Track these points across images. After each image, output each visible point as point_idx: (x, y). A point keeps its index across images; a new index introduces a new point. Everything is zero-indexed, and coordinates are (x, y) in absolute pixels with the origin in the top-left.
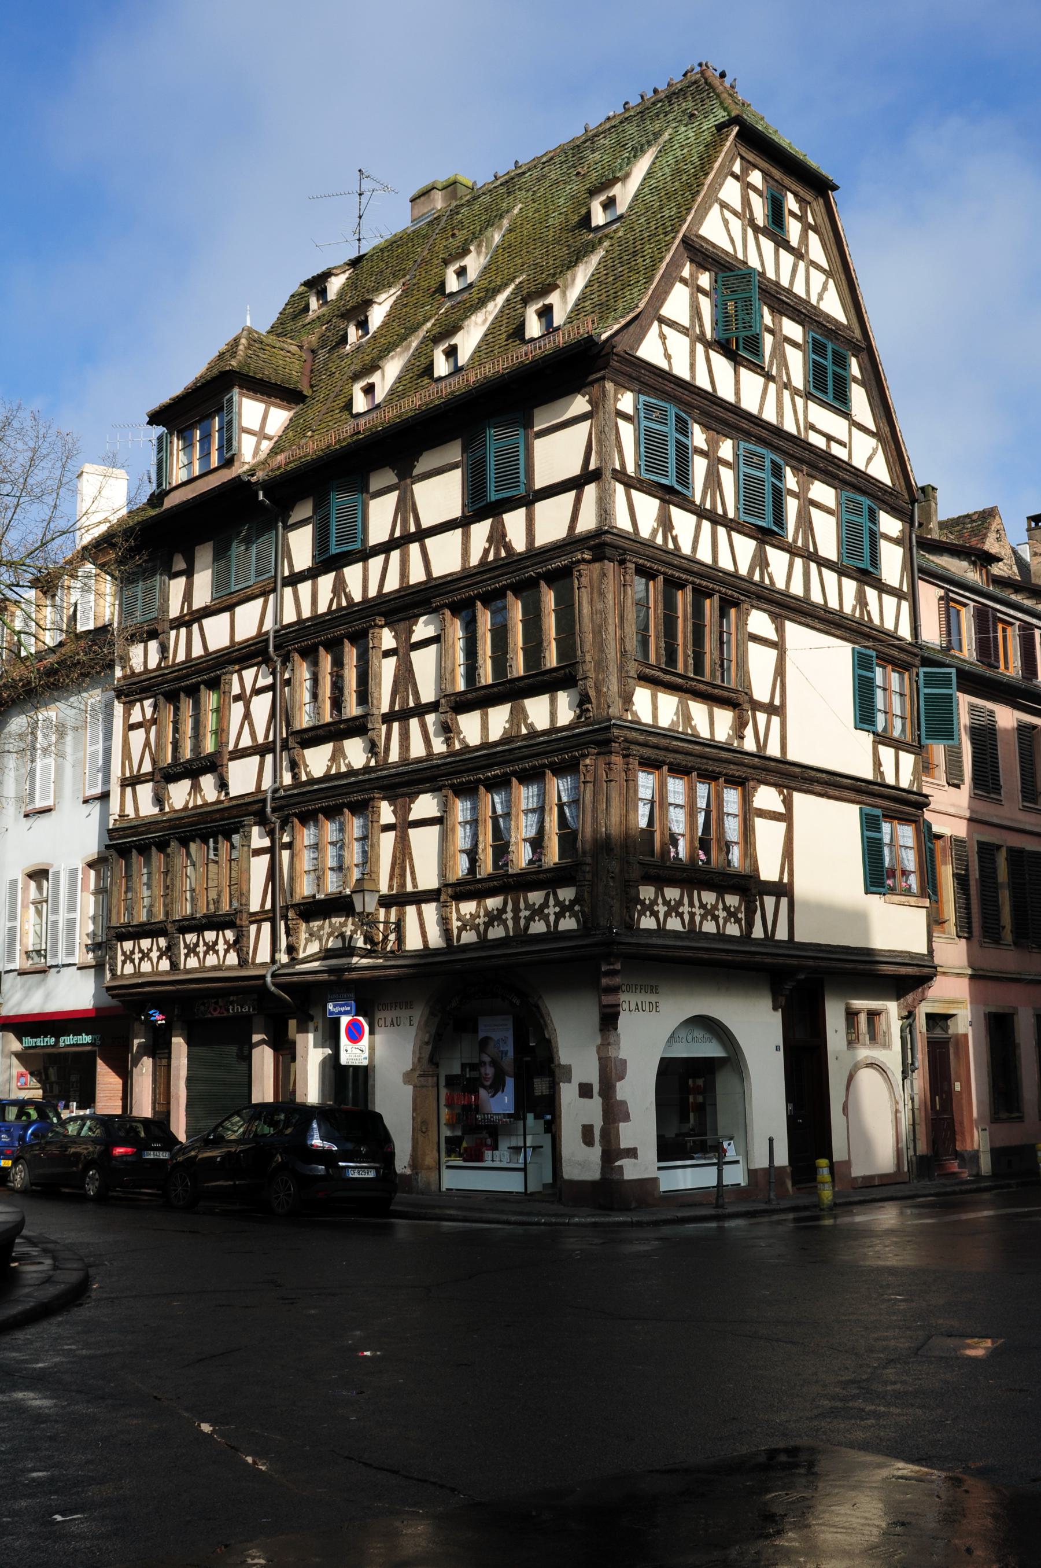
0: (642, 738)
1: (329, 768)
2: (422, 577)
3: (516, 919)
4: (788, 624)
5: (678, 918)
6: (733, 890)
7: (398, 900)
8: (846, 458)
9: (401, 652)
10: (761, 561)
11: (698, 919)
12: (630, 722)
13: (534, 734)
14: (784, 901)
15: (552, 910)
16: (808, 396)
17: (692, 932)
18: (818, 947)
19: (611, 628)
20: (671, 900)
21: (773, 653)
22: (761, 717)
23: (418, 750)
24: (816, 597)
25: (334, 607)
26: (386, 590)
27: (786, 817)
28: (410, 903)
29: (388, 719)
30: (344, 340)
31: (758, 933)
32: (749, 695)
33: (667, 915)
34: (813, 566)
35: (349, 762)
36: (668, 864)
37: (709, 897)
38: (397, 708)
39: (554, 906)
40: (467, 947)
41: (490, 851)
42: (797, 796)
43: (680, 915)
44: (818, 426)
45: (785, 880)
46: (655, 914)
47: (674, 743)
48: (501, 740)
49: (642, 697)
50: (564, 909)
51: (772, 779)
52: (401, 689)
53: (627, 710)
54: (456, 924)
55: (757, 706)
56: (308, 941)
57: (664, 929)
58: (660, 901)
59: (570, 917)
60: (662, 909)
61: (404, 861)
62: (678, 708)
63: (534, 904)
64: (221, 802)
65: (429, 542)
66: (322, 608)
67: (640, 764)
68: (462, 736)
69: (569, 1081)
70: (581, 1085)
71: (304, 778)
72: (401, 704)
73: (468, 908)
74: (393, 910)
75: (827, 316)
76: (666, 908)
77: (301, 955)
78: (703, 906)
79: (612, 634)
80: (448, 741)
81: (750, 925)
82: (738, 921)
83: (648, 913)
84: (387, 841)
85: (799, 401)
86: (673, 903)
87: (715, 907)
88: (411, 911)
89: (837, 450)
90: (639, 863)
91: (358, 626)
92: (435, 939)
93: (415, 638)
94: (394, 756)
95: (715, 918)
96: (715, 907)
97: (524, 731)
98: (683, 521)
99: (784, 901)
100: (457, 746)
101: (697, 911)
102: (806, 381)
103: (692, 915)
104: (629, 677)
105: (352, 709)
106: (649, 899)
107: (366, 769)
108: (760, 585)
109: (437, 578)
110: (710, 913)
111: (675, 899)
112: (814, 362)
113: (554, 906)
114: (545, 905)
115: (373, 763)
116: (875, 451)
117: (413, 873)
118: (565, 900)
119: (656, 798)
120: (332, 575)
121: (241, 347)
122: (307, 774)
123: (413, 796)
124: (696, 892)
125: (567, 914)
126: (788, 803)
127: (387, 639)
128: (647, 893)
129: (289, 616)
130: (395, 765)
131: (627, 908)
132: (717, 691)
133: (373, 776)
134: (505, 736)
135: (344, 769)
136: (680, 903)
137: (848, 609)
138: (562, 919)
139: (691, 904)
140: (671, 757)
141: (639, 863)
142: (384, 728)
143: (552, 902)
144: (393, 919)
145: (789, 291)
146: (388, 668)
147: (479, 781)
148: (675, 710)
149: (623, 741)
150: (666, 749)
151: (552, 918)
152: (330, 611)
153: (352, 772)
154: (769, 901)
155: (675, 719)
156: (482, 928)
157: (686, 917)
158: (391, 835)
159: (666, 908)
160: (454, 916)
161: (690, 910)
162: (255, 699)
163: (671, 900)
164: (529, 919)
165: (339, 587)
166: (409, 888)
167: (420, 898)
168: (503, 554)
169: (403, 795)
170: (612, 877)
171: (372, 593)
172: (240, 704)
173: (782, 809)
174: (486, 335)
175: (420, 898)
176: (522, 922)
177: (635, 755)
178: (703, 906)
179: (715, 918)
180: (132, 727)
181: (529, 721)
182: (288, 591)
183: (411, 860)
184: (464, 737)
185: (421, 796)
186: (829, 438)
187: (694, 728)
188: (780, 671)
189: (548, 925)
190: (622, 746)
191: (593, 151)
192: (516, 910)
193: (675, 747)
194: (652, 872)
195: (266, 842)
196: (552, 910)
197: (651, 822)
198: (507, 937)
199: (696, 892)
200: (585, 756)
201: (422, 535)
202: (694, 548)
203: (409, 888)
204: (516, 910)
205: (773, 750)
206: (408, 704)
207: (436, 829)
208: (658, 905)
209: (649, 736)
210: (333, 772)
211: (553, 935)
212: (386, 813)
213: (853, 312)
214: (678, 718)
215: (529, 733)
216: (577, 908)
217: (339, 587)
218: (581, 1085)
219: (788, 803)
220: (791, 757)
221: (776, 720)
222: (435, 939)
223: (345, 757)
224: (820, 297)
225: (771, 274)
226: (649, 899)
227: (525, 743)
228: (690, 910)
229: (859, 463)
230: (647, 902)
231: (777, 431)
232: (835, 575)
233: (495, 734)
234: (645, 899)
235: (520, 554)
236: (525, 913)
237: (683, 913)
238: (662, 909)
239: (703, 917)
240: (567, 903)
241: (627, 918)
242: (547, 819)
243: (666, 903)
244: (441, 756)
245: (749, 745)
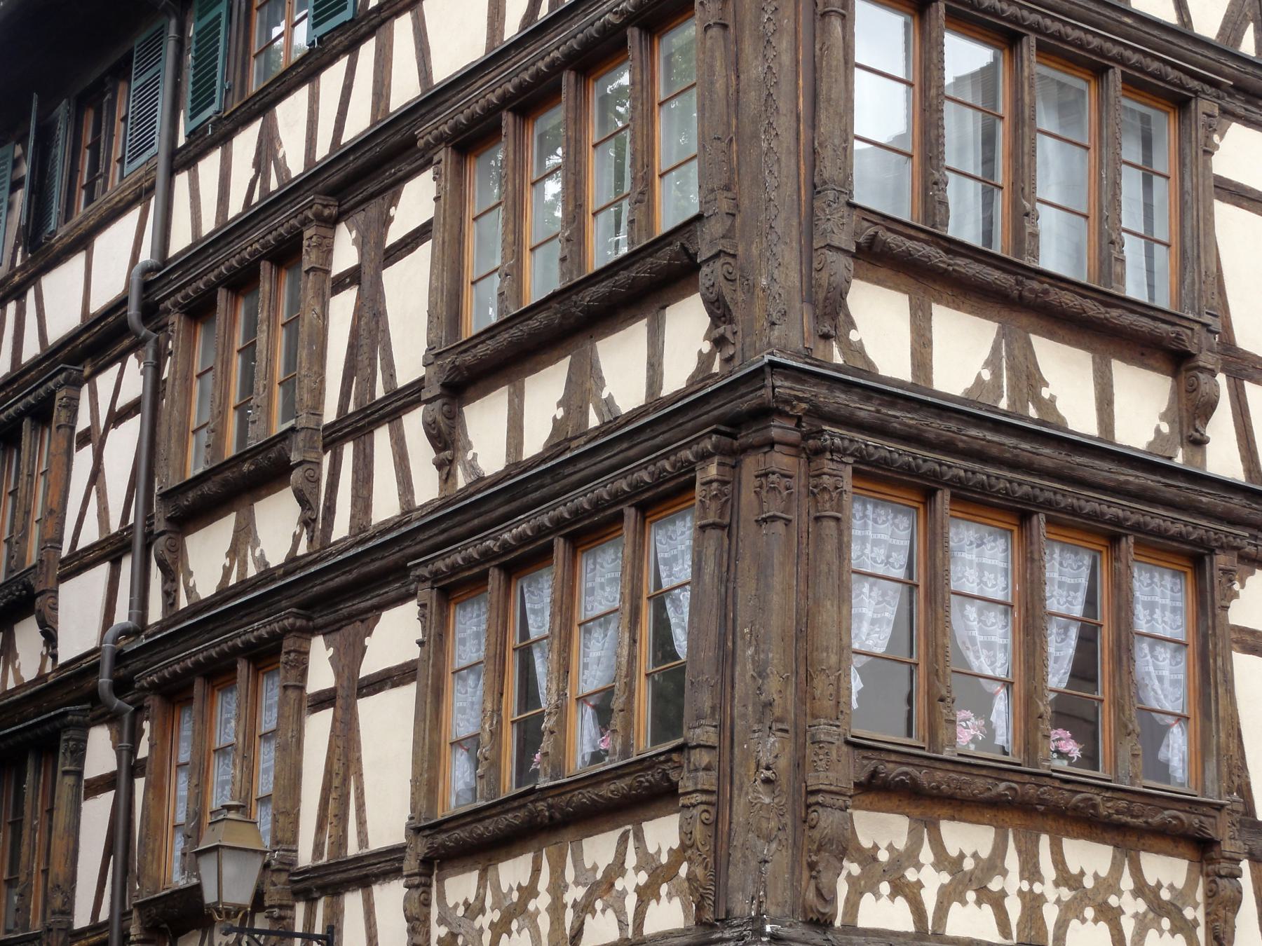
0: (866, 410)
5: (987, 909)
11: (1050, 914)
12: (838, 368)
19: (784, 124)
20: (962, 856)
29: (333, 438)
33: (947, 897)
35: (262, 555)
36: (946, 754)
38: (351, 409)
39: (637, 869)
47: (974, 432)
48: (546, 449)
50: (659, 875)
53: (826, 337)
57: (939, 936)
58: (926, 855)
59: (670, 896)
60: (931, 881)
61: (345, 781)
62: (996, 349)
63: (595, 868)
67: (857, 473)
68: (470, 456)
76: (945, 878)
78: (1066, 878)
79: (787, 138)
80: (445, 467)
83: (885, 887)
86: (968, 864)
87: (1110, 885)
90: (848, 743)
96: (1110, 885)
97: (594, 421)
101: (1047, 888)
103: (1033, 903)
104: (830, 247)
106: (890, 848)
111: (975, 855)
113: (637, 869)
114: (617, 868)
118: (659, 851)
119: (919, 578)
123: (369, 618)
124: (1045, 841)
125: (664, 889)
131: (812, 866)
132: (1115, 313)
134: (556, 440)
136: (994, 865)
138: (653, 903)
139: (1031, 871)
140: (958, 467)
141: (848, 743)
143: (631, 859)
148: (986, 352)
149: (808, 413)
150: (947, 447)
155: (987, 375)
157: (1014, 908)
159: (945, 878)
161: (1025, 886)
163: (962, 856)
170: (767, 781)
171: (323, 150)
177: (843, 451)
178: (1066, 878)
181: (605, 395)
184: (475, 455)
185: (387, 616)
187: (1048, 405)
190: (805, 427)
193: (977, 445)
194: (893, 770)
199: (1045, 841)
200: (704, 456)
204: (557, 888)
206: (373, 394)
208: (918, 866)
209: (892, 405)
214: (996, 375)
215: (604, 424)
216: (683, 870)
226: (890, 848)
228: (1025, 886)
230: (883, 856)
234: (876, 847)
236: (575, 894)
237: (1003, 894)
238: (931, 881)
239: (1070, 911)
240: (664, 859)
241: (811, 895)
243: (943, 861)
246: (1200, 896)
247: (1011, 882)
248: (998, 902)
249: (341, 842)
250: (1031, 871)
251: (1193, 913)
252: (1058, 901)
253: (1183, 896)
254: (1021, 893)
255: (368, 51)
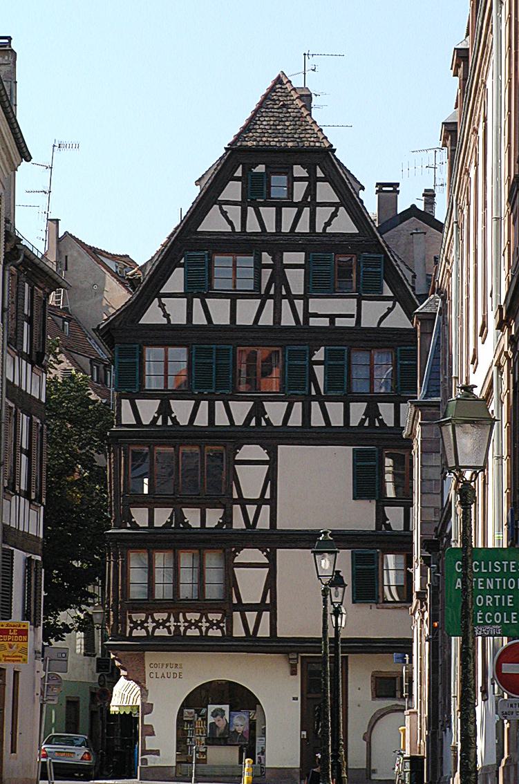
6: (215, 610)
11: (182, 629)
14: (266, 615)
37: (192, 617)
45: (268, 601)
55: (243, 502)
99: (266, 615)
103: (177, 627)
106: (141, 620)
110: (196, 625)
128: (139, 617)
139: (177, 620)
157: (172, 629)
230: (139, 622)
246: (225, 621)
247: (172, 623)
248: (168, 628)
250: (177, 620)
252: (184, 626)
253: (221, 621)
254: (174, 625)
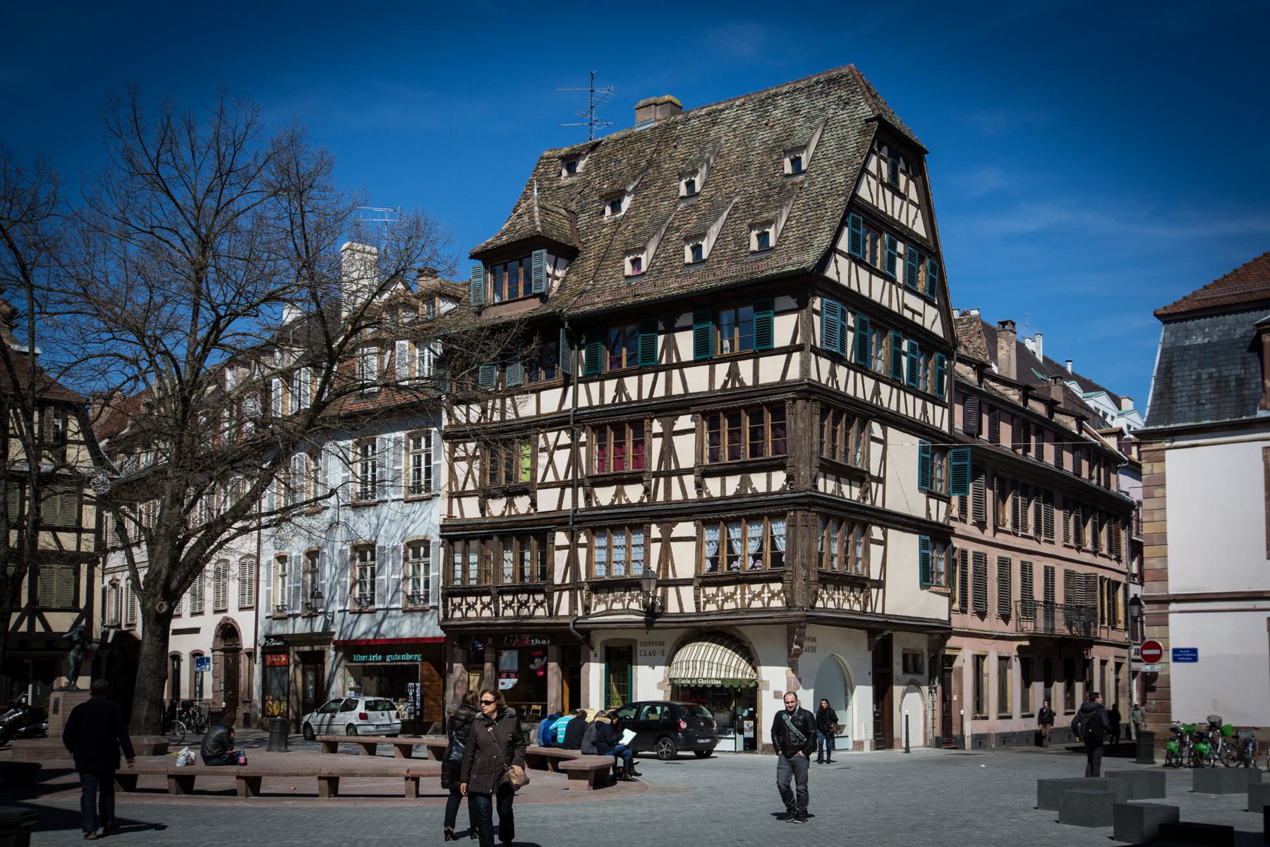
1: (613, 501)
2: (682, 392)
3: (743, 599)
4: (889, 429)
7: (665, 584)
8: (921, 324)
9: (666, 435)
10: (877, 392)
13: (756, 494)
14: (881, 591)
15: (766, 595)
16: (906, 288)
17: (839, 610)
18: (895, 617)
21: (881, 447)
22: (874, 485)
23: (677, 495)
24: (903, 411)
25: (617, 401)
26: (655, 395)
27: (883, 543)
28: (672, 586)
29: (657, 475)
30: (603, 212)
31: (869, 610)
32: (869, 473)
34: (902, 393)
40: (708, 614)
41: (725, 559)
42: (890, 531)
43: (833, 599)
44: (910, 306)
46: (822, 599)
49: (821, 482)
51: (879, 522)
52: (666, 457)
54: (702, 599)
56: (596, 604)
61: (667, 560)
64: (532, 514)
65: (686, 370)
66: (608, 400)
69: (768, 689)
70: (775, 692)
71: (594, 505)
72: (665, 467)
73: (711, 591)
74: (659, 590)
75: (917, 234)
77: (592, 612)
81: (866, 605)
82: (859, 602)
84: (656, 549)
85: (900, 291)
88: (672, 591)
89: (918, 320)
91: (637, 416)
92: (690, 607)
93: (676, 428)
94: (660, 497)
95: (849, 601)
97: (749, 492)
98: (841, 371)
100: (705, 496)
101: (842, 597)
102: (904, 279)
103: (839, 599)
105: (629, 467)
107: (640, 504)
108: (876, 407)
109: (691, 394)
112: (909, 265)
114: (762, 592)
115: (645, 500)
116: (936, 316)
117: (673, 568)
120: (615, 381)
121: (537, 214)
122: (597, 503)
126: (885, 535)
127: (657, 427)
129: (583, 402)
130: (661, 504)
133: (646, 509)
135: (624, 502)
137: (917, 417)
142: (653, 480)
144: (659, 594)
145: (898, 222)
146: (657, 444)
147: (721, 519)
151: (766, 600)
152: (613, 403)
153: (630, 505)
154: (874, 591)
156: (720, 603)
158: (659, 545)
160: (702, 595)
162: (556, 452)
164: (751, 600)
165: (620, 389)
166: (671, 576)
167: (678, 583)
168: (737, 385)
169: (667, 522)
171: (645, 395)
172: (546, 454)
173: (882, 538)
174: (717, 239)
175: (678, 583)
176: (747, 601)
179: (849, 601)
180: (457, 459)
182: (582, 387)
183: (672, 560)
186: (914, 312)
188: (884, 458)
189: (763, 604)
191: (775, 108)
192: (743, 594)
195: (567, 542)
196: (766, 595)
197: (822, 549)
198: (737, 609)
201: (681, 365)
202: (846, 387)
203: (671, 576)
204: (743, 594)
205: (879, 504)
207: (693, 544)
210: (616, 503)
211: (766, 609)
212: (655, 532)
213: (929, 229)
217: (620, 389)
218: (775, 692)
219: (885, 535)
220: (888, 507)
221: (881, 486)
222: (690, 607)
223: (625, 495)
224: (914, 223)
225: (889, 213)
227: (750, 499)
229: (928, 326)
231: (888, 312)
232: (912, 397)
233: (730, 491)
235: (749, 387)
238: (825, 596)
239: (844, 600)
242: (765, 544)
244: (693, 501)
245: (868, 502)
249: (666, 574)
251: (861, 599)
255: (662, 375)
